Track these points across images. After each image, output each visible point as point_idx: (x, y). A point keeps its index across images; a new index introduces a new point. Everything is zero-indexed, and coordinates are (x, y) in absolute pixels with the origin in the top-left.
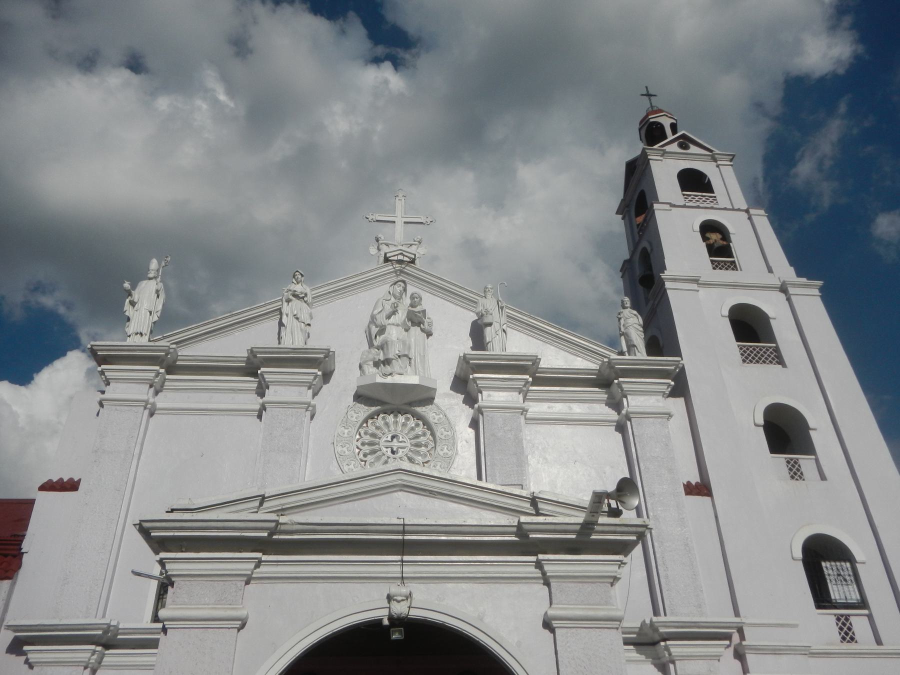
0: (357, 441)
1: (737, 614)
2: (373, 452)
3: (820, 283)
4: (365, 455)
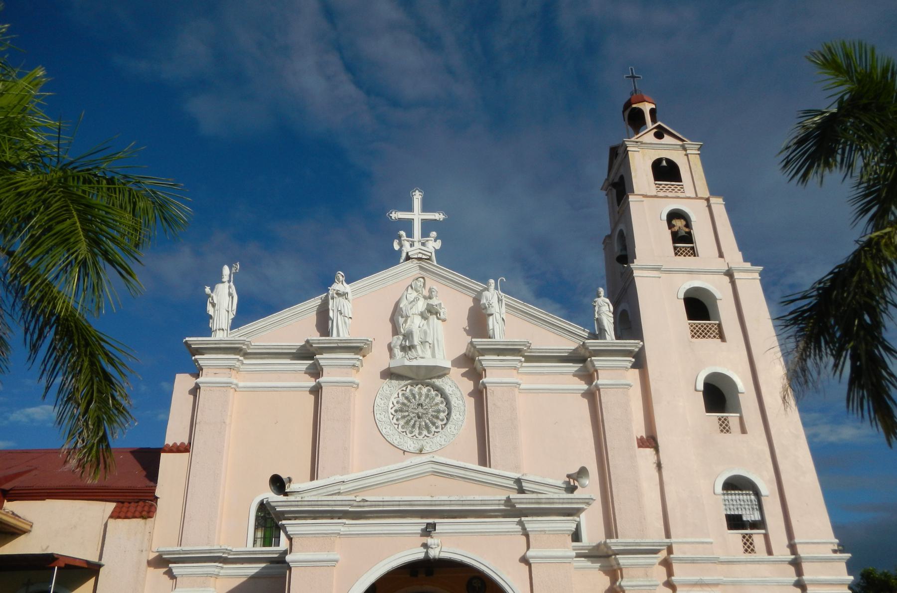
0: (392, 408)
1: (668, 535)
3: (761, 268)
4: (397, 420)
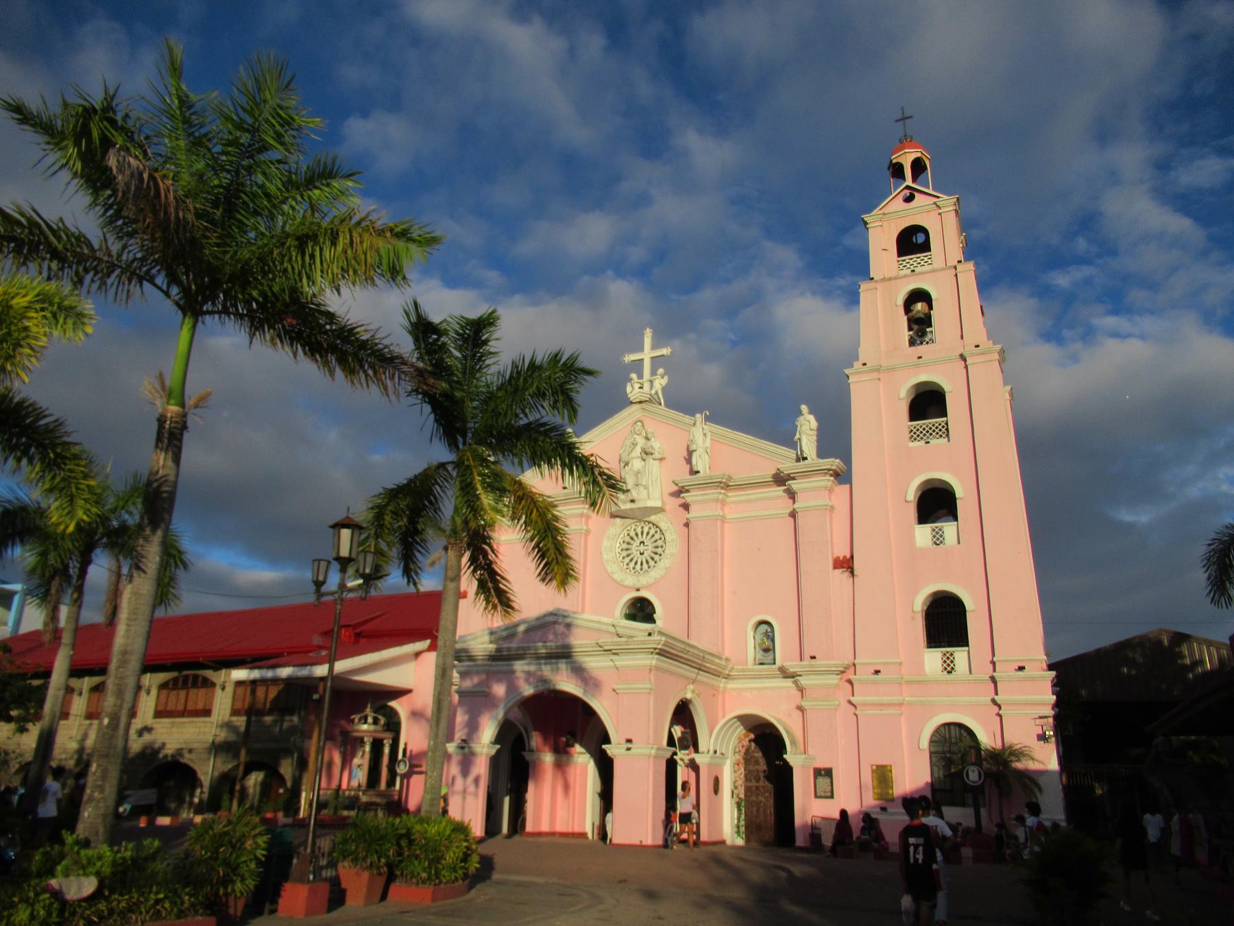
2: (628, 555)
